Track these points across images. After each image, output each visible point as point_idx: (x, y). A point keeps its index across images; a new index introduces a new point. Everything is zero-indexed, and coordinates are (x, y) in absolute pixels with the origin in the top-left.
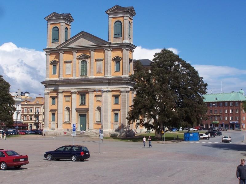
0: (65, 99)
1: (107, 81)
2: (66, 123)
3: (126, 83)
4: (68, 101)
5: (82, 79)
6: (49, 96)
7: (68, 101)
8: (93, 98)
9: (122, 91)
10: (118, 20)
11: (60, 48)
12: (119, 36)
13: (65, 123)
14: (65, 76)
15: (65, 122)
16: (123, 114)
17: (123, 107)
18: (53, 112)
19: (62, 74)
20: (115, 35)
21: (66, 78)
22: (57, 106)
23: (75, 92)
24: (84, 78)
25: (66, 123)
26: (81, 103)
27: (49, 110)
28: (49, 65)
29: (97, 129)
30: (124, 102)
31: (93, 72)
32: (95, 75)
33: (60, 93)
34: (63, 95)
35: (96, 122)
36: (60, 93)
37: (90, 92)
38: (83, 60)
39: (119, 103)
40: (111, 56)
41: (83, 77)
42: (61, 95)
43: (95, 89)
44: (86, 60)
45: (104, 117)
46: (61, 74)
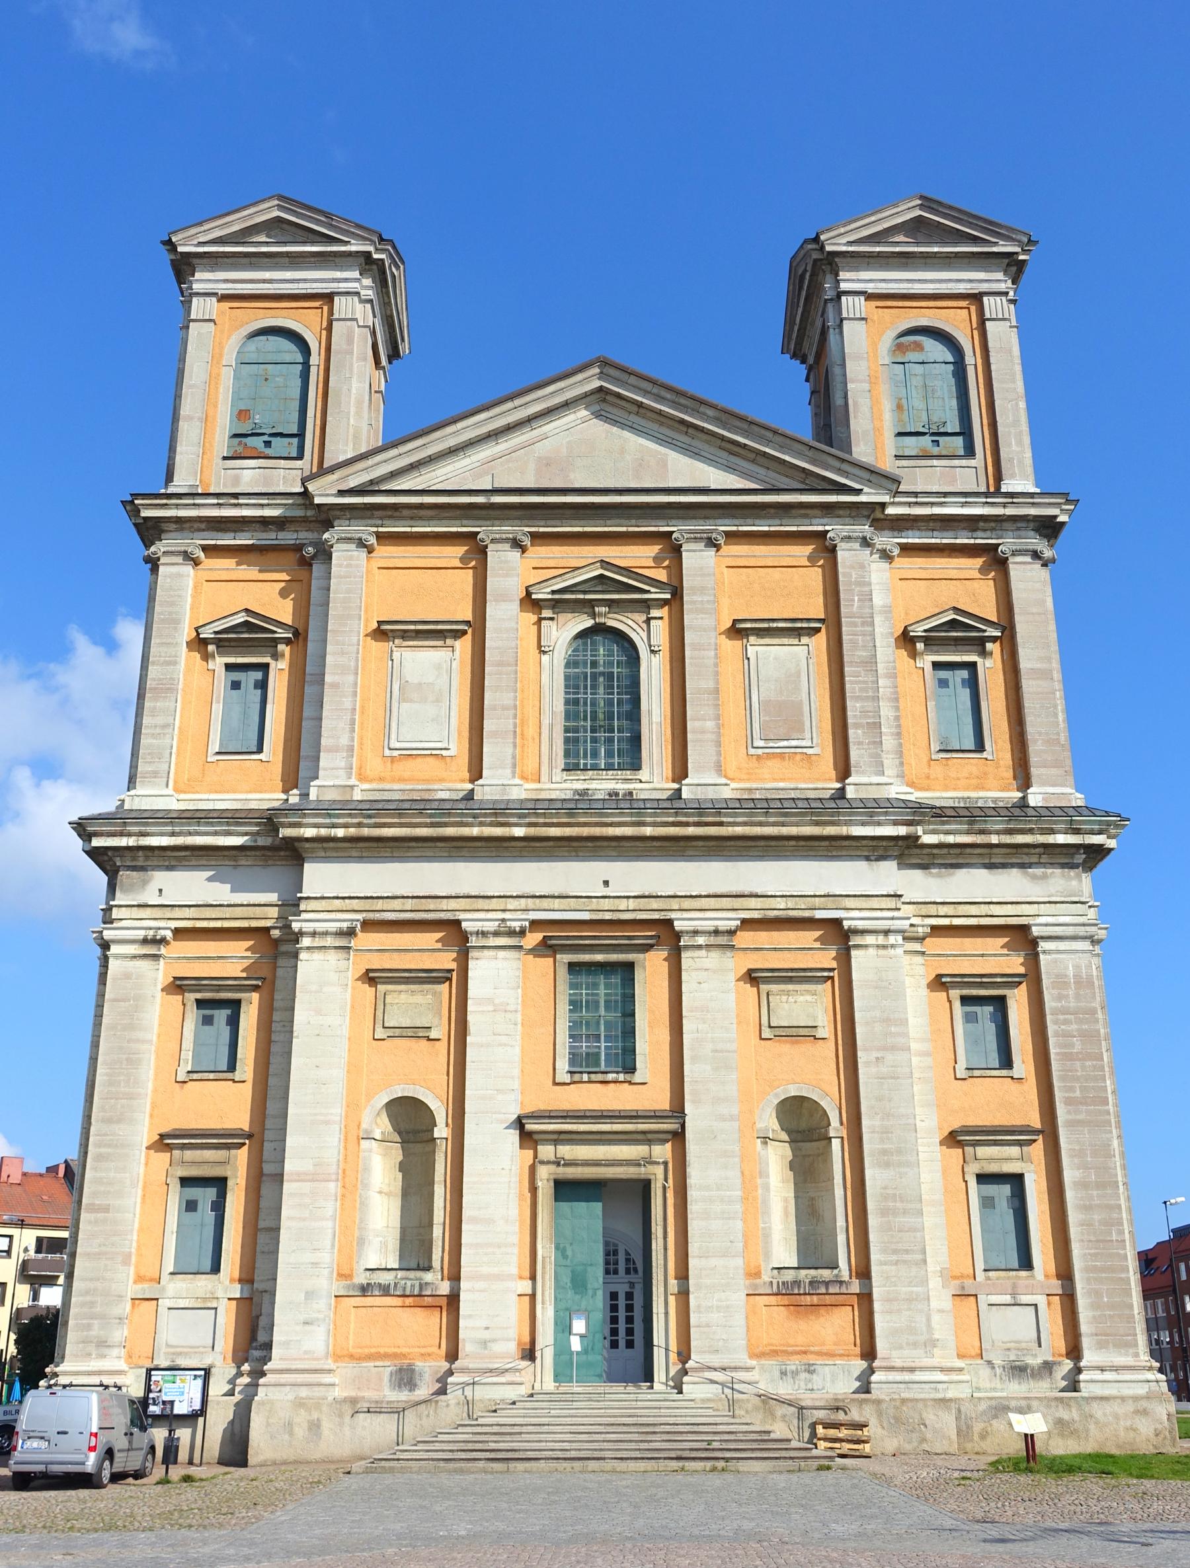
0: (380, 1007)
1: (896, 823)
2: (385, 1291)
3: (1080, 858)
4: (418, 1033)
5: (581, 803)
6: (159, 974)
7: (418, 1033)
8: (732, 996)
9: (1042, 938)
10: (924, 322)
11: (341, 493)
12: (935, 451)
13: (365, 1290)
14: (375, 766)
15: (361, 1278)
16: (1082, 1185)
17: (1068, 1102)
18: (204, 1161)
19: (344, 741)
20: (900, 438)
21: (395, 790)
22: (247, 1090)
23: (511, 933)
24: (613, 794)
25: (385, 1291)
26: (574, 1059)
27: (145, 1134)
28: (186, 658)
29: (793, 1364)
30: (1078, 1047)
31: (718, 744)
32: (731, 774)
33: (314, 934)
34: (355, 966)
35: (766, 1277)
36: (314, 934)
37: (696, 933)
38: (589, 623)
39: (1023, 1062)
40: (888, 611)
41: (602, 784)
42: (333, 957)
43: (753, 903)
44: (628, 623)
45: (884, 1212)
46: (335, 749)
